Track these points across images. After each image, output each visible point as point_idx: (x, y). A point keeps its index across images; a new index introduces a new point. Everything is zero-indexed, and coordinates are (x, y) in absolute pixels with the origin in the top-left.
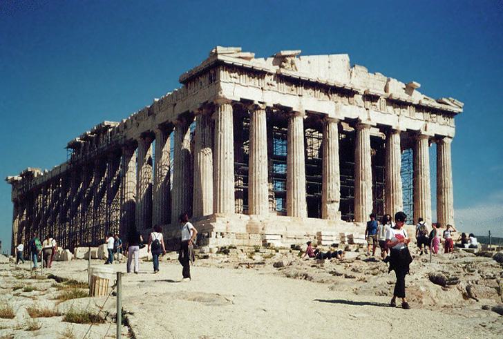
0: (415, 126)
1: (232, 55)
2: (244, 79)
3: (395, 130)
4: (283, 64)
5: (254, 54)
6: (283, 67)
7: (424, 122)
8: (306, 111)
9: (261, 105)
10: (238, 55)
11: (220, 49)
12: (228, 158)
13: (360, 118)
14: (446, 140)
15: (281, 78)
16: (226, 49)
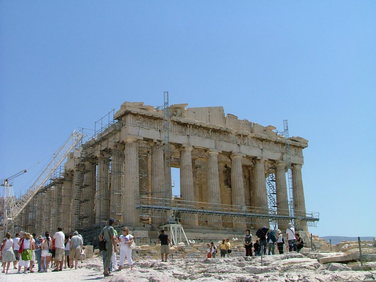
0: (276, 156)
6: (175, 116)
8: (193, 146)
9: (158, 143)
13: (234, 151)
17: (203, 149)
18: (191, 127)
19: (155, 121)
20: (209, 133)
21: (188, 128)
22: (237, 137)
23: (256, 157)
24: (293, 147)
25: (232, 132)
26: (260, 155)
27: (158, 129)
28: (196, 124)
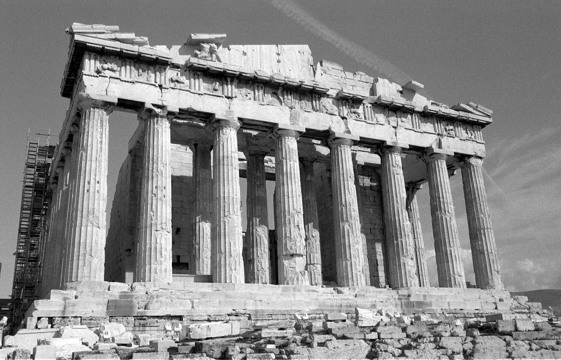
1: (99, 36)
2: (128, 72)
3: (391, 147)
4: (198, 52)
5: (146, 39)
6: (196, 56)
7: (436, 137)
8: (240, 119)
9: (158, 111)
10: (113, 36)
11: (77, 27)
12: (91, 190)
13: (333, 130)
14: (473, 161)
15: (194, 71)
16: (89, 26)
17: (266, 127)
18: (236, 82)
19: (152, 68)
20: (277, 94)
21: (229, 83)
22: (340, 103)
23: (383, 142)
24: (461, 123)
25: (328, 93)
26: (392, 138)
27: (156, 82)
28: (243, 74)
